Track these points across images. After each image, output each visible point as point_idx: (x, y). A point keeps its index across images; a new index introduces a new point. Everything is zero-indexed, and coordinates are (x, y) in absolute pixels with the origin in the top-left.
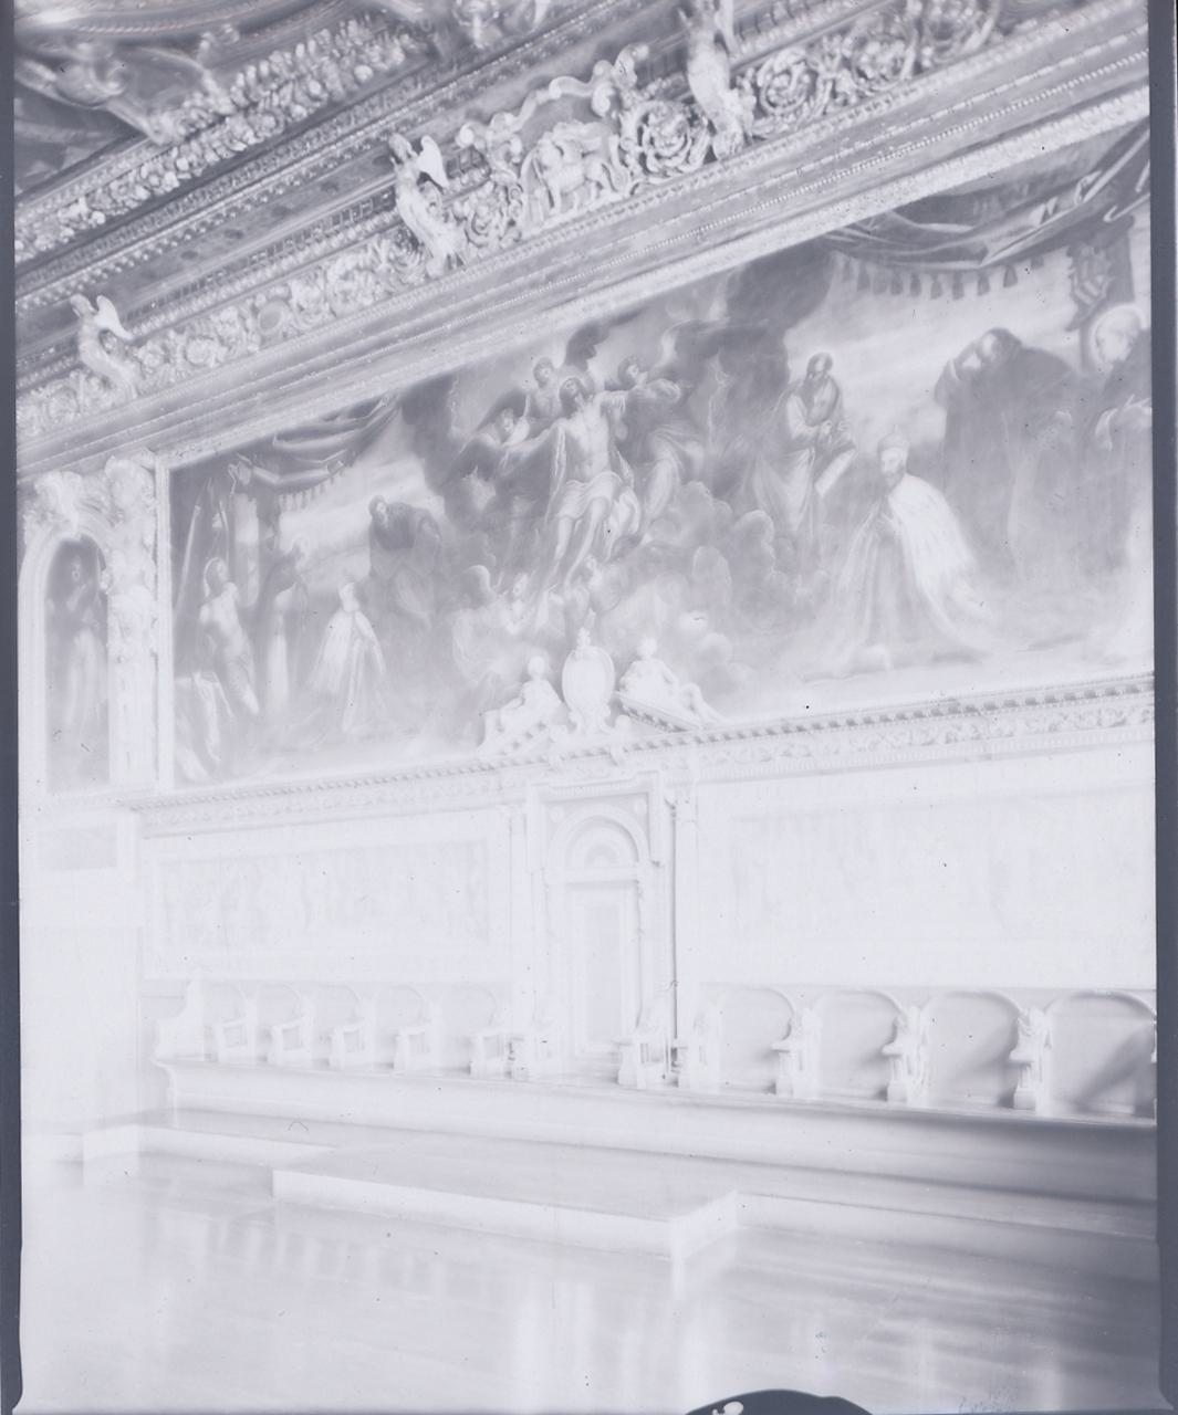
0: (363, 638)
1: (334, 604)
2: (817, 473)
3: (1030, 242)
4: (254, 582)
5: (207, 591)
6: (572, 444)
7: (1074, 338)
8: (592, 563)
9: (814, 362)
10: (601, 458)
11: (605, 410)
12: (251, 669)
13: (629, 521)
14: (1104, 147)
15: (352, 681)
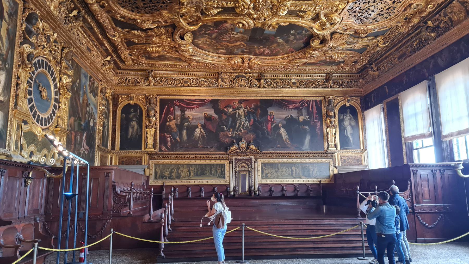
1: (197, 127)
2: (272, 125)
4: (179, 121)
6: (239, 114)
8: (242, 129)
10: (243, 117)
11: (244, 110)
12: (178, 134)
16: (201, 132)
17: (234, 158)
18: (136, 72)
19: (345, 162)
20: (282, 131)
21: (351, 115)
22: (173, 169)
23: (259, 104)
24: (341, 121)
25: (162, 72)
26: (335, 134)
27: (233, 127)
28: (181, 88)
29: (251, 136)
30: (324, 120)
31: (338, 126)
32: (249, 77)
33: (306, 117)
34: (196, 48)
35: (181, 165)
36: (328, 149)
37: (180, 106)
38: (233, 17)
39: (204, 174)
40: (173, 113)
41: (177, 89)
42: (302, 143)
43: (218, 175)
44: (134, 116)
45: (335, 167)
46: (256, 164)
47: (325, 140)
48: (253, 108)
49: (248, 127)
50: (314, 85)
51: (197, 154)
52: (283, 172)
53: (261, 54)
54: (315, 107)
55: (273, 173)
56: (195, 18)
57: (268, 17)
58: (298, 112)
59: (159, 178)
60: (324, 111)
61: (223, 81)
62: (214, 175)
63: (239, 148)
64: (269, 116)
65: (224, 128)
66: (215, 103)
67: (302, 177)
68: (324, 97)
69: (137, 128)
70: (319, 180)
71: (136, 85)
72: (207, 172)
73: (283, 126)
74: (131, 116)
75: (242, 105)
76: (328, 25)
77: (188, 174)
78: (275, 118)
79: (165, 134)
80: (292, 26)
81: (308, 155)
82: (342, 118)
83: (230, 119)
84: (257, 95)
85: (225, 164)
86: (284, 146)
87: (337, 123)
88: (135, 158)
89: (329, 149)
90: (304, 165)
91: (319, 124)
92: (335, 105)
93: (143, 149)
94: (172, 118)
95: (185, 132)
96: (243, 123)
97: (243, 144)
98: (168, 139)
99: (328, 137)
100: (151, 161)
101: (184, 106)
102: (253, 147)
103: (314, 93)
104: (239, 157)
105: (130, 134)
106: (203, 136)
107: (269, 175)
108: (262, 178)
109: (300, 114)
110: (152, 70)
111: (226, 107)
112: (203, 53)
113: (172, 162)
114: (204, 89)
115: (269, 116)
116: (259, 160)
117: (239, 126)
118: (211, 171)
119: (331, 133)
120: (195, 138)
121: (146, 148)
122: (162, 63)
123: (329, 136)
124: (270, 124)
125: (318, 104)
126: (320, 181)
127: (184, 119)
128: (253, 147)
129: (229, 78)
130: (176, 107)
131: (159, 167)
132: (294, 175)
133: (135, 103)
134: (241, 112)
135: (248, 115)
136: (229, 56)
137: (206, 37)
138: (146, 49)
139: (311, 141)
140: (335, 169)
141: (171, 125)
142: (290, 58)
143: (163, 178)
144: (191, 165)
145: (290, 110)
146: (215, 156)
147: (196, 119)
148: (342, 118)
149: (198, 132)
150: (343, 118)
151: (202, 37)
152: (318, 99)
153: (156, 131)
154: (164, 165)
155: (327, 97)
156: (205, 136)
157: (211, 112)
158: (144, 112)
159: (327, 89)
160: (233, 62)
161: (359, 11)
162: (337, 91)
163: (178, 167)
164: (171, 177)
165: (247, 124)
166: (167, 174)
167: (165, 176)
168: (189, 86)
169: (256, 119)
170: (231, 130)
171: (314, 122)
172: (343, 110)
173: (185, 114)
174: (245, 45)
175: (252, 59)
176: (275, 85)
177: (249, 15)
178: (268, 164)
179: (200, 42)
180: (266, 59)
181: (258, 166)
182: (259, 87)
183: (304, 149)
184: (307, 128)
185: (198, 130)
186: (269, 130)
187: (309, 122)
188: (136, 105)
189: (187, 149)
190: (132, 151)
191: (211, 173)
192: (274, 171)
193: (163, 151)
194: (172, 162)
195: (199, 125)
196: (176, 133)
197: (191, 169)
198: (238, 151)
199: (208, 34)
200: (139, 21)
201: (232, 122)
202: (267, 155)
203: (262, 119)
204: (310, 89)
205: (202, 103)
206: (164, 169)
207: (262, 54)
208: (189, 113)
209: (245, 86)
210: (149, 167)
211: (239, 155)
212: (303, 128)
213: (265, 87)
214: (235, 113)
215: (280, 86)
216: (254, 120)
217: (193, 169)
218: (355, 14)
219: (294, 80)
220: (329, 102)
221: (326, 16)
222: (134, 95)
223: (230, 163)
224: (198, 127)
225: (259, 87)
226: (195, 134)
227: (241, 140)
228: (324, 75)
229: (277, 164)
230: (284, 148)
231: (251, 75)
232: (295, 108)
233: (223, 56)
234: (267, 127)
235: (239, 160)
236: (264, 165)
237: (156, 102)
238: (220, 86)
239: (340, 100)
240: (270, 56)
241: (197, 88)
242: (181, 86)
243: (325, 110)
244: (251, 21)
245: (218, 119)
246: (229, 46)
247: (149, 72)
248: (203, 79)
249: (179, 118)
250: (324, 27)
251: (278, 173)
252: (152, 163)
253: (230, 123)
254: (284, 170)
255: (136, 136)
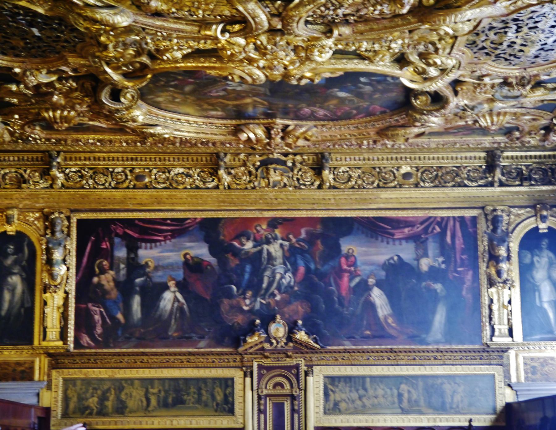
0: (178, 301)
1: (166, 287)
2: (351, 280)
3: (405, 236)
4: (123, 272)
5: (97, 270)
6: (269, 253)
7: (416, 262)
8: (276, 292)
9: (349, 249)
10: (280, 260)
11: (281, 245)
12: (121, 305)
13: (290, 282)
14: (421, 220)
15: (173, 317)
16: (176, 299)
17: (255, 365)
18: (21, 155)
19: (534, 373)
20: (378, 296)
21: (551, 255)
22: (109, 390)
23: (319, 229)
24: (525, 270)
25: (82, 156)
26: (510, 302)
27: (255, 286)
28: (129, 193)
29: (299, 308)
30: (483, 266)
31: (517, 284)
32: (294, 164)
33: (435, 261)
34: (155, 110)
35: (126, 380)
36: (491, 340)
37: (124, 236)
38: (216, 65)
39: (183, 402)
40: (109, 255)
41: (118, 194)
42: (425, 324)
43: (217, 404)
44: (16, 262)
45: (509, 385)
46: (310, 379)
47: (486, 320)
48: (303, 240)
49: (292, 288)
50: (458, 180)
51: (166, 354)
52: (376, 397)
53: (310, 117)
54: (459, 234)
55: (353, 402)
56: (138, 65)
57: (292, 62)
58: (417, 249)
59: (74, 413)
60: (483, 245)
61: (229, 174)
62: (206, 405)
63: (268, 340)
64: (343, 260)
65: (231, 289)
66: (209, 229)
67: (424, 409)
68: (483, 208)
69: (23, 292)
70: (468, 417)
71: (20, 187)
72: (190, 398)
73: (379, 284)
74: (9, 261)
75: (277, 232)
76: (433, 72)
77: (145, 403)
78: (359, 263)
79: (90, 305)
80: (351, 77)
81: (439, 356)
82: (527, 260)
83: (248, 268)
84: (315, 207)
85: (232, 379)
86: (380, 334)
87: (515, 275)
88: (18, 364)
89: (494, 339)
90: (430, 381)
91: (469, 276)
92: (511, 228)
93: (36, 342)
94: (106, 267)
95: (136, 301)
96: (278, 276)
97: (278, 329)
98: (97, 317)
99: (491, 310)
100: (54, 373)
101: (136, 235)
102: (301, 336)
103: (456, 199)
104: (267, 362)
105: (6, 306)
106: (181, 309)
107: (343, 406)
108: (325, 413)
109: (420, 252)
110: (58, 153)
111: (237, 237)
112: (172, 118)
113: (104, 374)
114: (184, 194)
115: (343, 260)
116: (316, 369)
117: (270, 284)
118: (200, 395)
119: (499, 300)
120: (160, 316)
121: (44, 339)
122: (80, 137)
123: (495, 307)
124: (346, 279)
125: (468, 226)
126: (470, 421)
127: (135, 267)
128: (301, 336)
129: (245, 165)
130: (117, 240)
131: (75, 385)
132: (405, 404)
133: (18, 232)
134: (275, 249)
135: (291, 256)
136: (234, 122)
137: (170, 91)
138: (39, 114)
139: (449, 321)
140: (508, 391)
141: (104, 282)
142: (379, 125)
143: (83, 413)
144: (151, 381)
145: (397, 242)
146: (211, 358)
147: (164, 267)
148: (527, 260)
149: (169, 299)
150: (532, 263)
151: (162, 92)
152: (469, 214)
153: (66, 299)
154: (87, 382)
155: (490, 208)
156: (185, 307)
157: (201, 251)
158: (39, 253)
159: (490, 189)
160: (244, 137)
161: (493, 46)
162: (517, 193)
163: (120, 385)
164: (102, 409)
165: (288, 279)
166: (93, 402)
167: (88, 407)
168: (146, 187)
169: (312, 266)
170: (249, 294)
171: (456, 272)
172: (531, 240)
173: (136, 255)
174: (265, 103)
175: (290, 128)
176: (360, 182)
177: (251, 61)
178: (339, 378)
179: (160, 99)
180: (323, 126)
181: (315, 384)
182: (320, 187)
183: (430, 339)
184: (438, 287)
185: (168, 296)
186: (344, 293)
187: (445, 271)
188: (20, 236)
189: (142, 341)
190: (10, 347)
191: (199, 401)
192: (355, 395)
193: (83, 347)
194: (104, 374)
195: (171, 284)
196: (115, 302)
197: (151, 390)
198: (267, 346)
199: (175, 86)
200: (17, 70)
201: (252, 274)
202: (337, 355)
203: (326, 267)
204: (446, 190)
205: (179, 229)
206: (87, 391)
207: (312, 117)
208: (147, 254)
209: (285, 185)
210: (49, 387)
211: (267, 357)
212: (428, 289)
213: (334, 188)
214: (260, 252)
215: (373, 183)
216: (308, 270)
217: (155, 391)
218: (486, 51)
219: (405, 169)
220: (495, 221)
221: (422, 56)
222: (15, 212)
223: (245, 376)
224: (167, 288)
225: (320, 187)
226: (162, 304)
227: (273, 319)
228: (483, 155)
229: (363, 378)
230: (382, 337)
231: (298, 158)
232: (408, 239)
233: (222, 122)
234: (338, 286)
235: (269, 369)
236: (331, 380)
237: (69, 227)
238: (221, 187)
239: (523, 217)
240: (332, 120)
241: (166, 193)
242: (128, 188)
243: (486, 243)
244: (258, 72)
245: (217, 268)
246: (228, 105)
247: (50, 156)
248: (181, 170)
249: (122, 266)
250: (425, 76)
251: (364, 400)
252: (58, 377)
253: (247, 276)
254: (380, 392)
255: (19, 309)
